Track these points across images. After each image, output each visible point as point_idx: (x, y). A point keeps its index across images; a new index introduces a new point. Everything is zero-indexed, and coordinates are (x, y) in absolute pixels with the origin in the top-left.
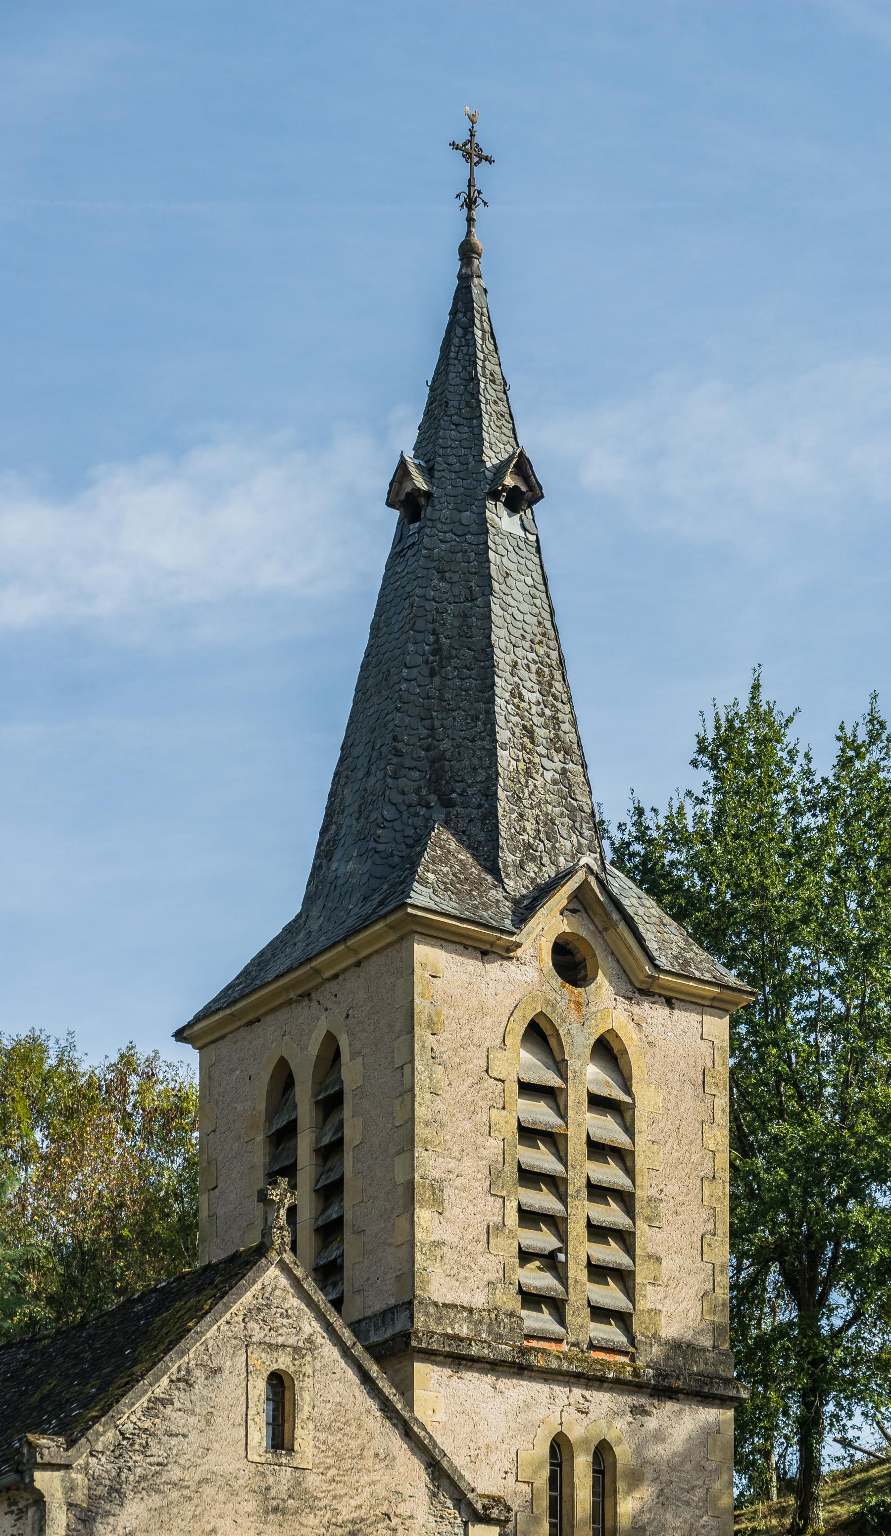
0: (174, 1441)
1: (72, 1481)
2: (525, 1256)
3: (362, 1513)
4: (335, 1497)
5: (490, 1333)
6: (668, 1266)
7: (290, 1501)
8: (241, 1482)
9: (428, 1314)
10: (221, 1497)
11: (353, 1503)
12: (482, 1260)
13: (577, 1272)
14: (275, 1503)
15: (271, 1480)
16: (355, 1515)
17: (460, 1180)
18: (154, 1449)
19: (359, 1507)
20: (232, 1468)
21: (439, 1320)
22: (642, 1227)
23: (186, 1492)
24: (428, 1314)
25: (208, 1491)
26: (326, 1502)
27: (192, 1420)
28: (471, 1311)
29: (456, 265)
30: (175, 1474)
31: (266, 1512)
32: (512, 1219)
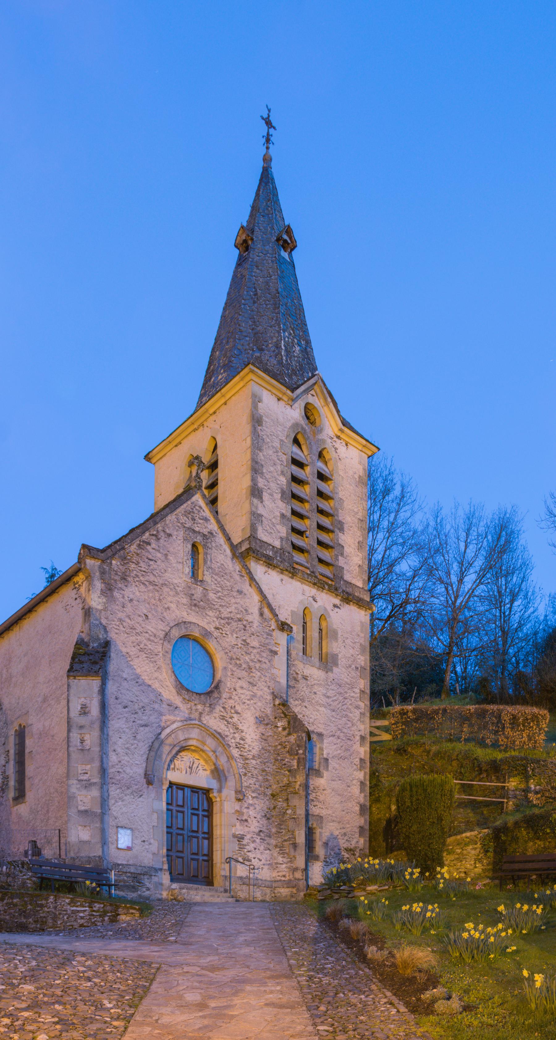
0: (151, 563)
1: (104, 569)
3: (232, 615)
4: (220, 606)
5: (281, 558)
7: (202, 603)
8: (180, 589)
9: (256, 543)
10: (171, 593)
11: (228, 610)
12: (278, 527)
14: (195, 602)
15: (193, 592)
16: (229, 615)
17: (269, 491)
18: (142, 564)
19: (231, 612)
20: (176, 581)
21: (261, 547)
23: (156, 587)
24: (256, 543)
25: (165, 589)
26: (216, 607)
27: (159, 555)
28: (273, 547)
29: (261, 164)
30: (152, 578)
31: (191, 605)
32: (289, 514)
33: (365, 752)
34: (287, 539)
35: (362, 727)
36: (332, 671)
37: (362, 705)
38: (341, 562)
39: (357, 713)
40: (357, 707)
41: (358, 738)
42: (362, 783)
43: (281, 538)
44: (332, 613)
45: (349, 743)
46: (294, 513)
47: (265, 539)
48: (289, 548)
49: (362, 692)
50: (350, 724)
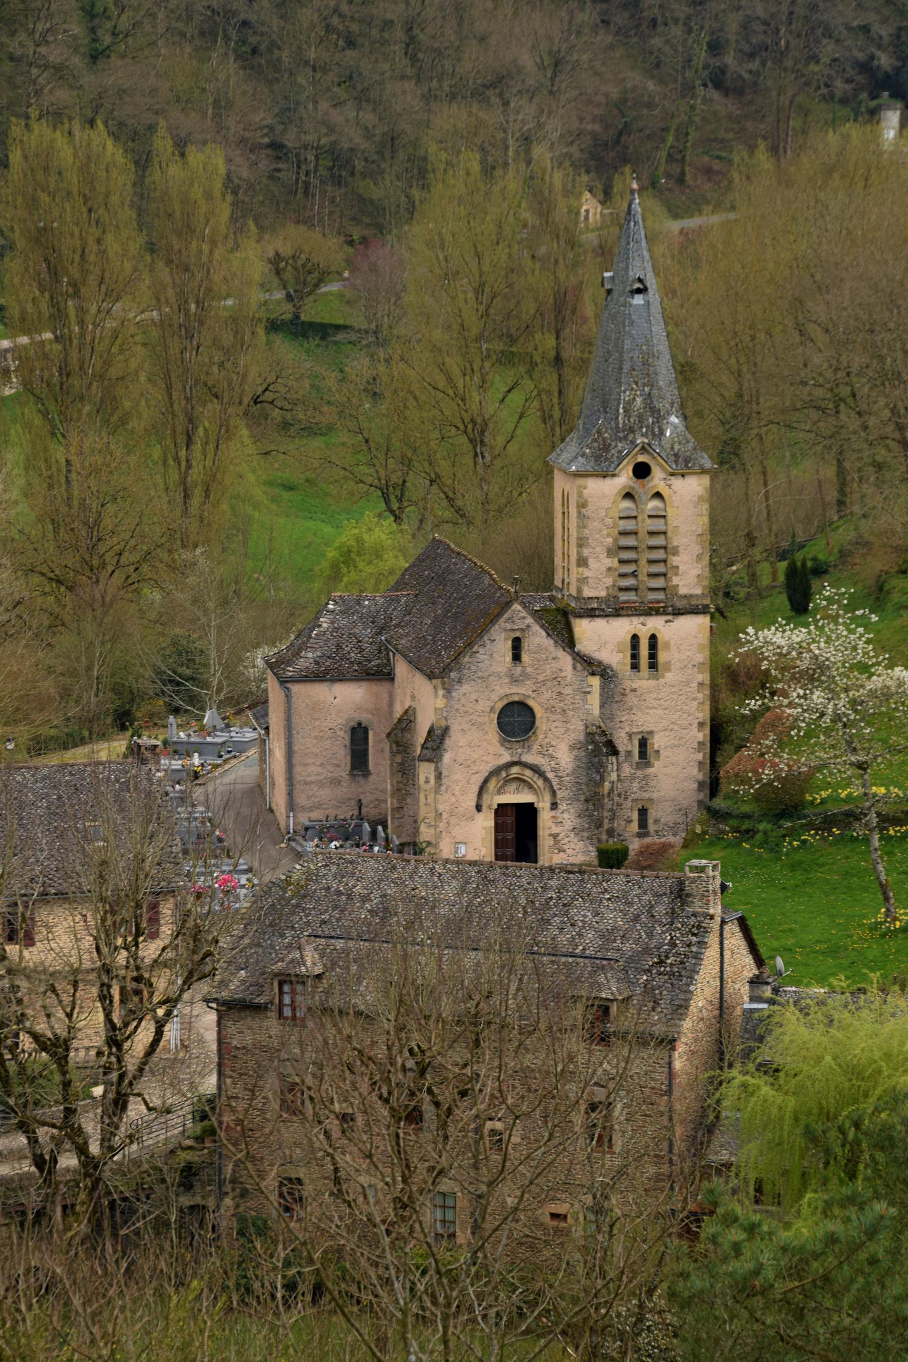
2: (623, 576)
6: (682, 568)
13: (643, 577)
22: (670, 557)
33: (705, 736)
34: (614, 586)
35: (701, 715)
36: (663, 677)
37: (700, 696)
38: (675, 580)
39: (695, 704)
40: (694, 699)
41: (695, 725)
42: (700, 763)
43: (607, 588)
44: (662, 629)
45: (685, 732)
46: (621, 562)
47: (591, 595)
48: (615, 592)
49: (701, 684)
50: (685, 716)
